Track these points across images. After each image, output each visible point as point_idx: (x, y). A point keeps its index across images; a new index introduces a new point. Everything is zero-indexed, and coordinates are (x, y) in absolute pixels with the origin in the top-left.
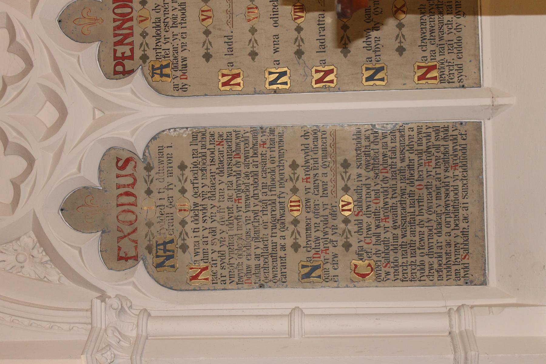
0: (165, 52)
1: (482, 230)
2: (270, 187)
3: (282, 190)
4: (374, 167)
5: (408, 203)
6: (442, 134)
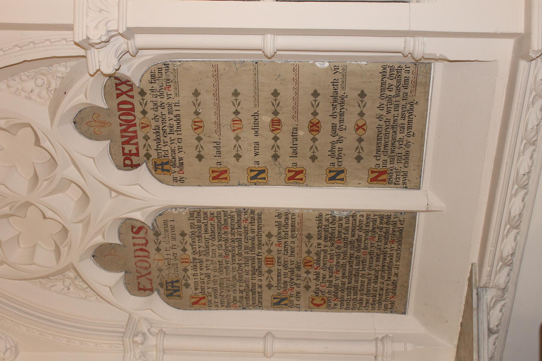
1: (408, 282)
2: (251, 249)
3: (260, 251)
4: (331, 239)
5: (355, 263)
6: (385, 220)
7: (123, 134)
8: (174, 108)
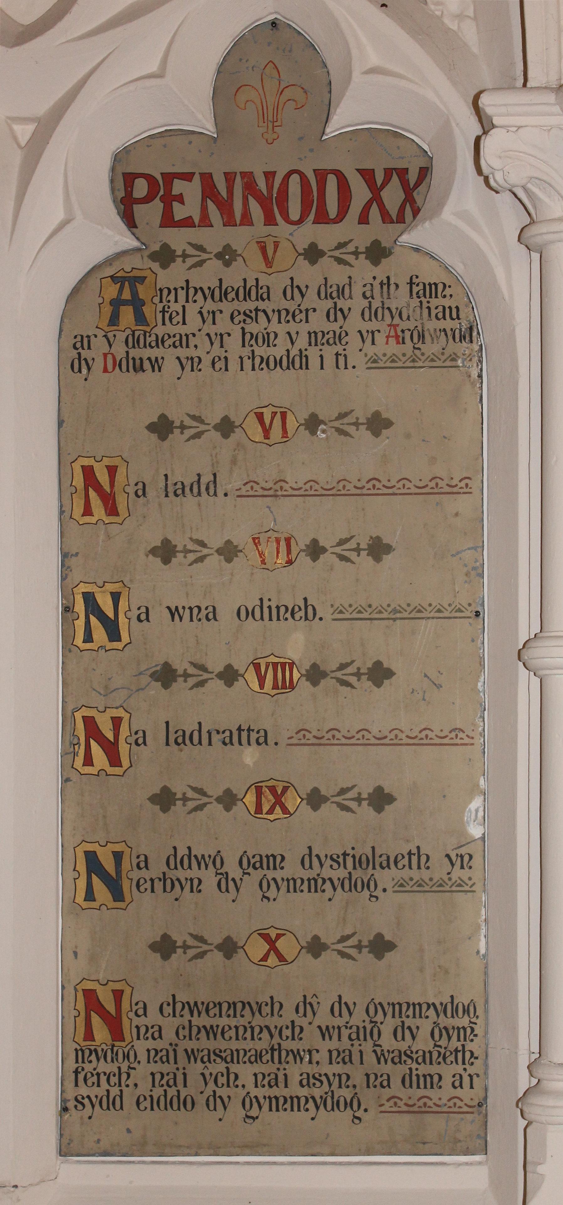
0: (178, 314)
7: (238, 179)
8: (329, 352)
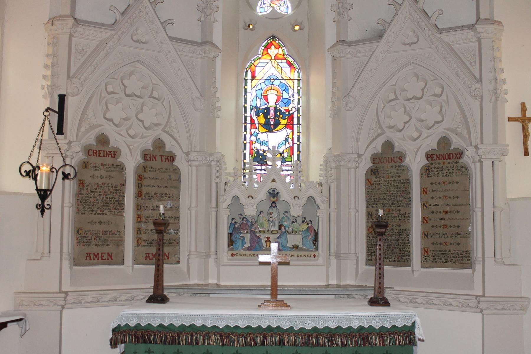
5: (389, 244)
8: (451, 174)
